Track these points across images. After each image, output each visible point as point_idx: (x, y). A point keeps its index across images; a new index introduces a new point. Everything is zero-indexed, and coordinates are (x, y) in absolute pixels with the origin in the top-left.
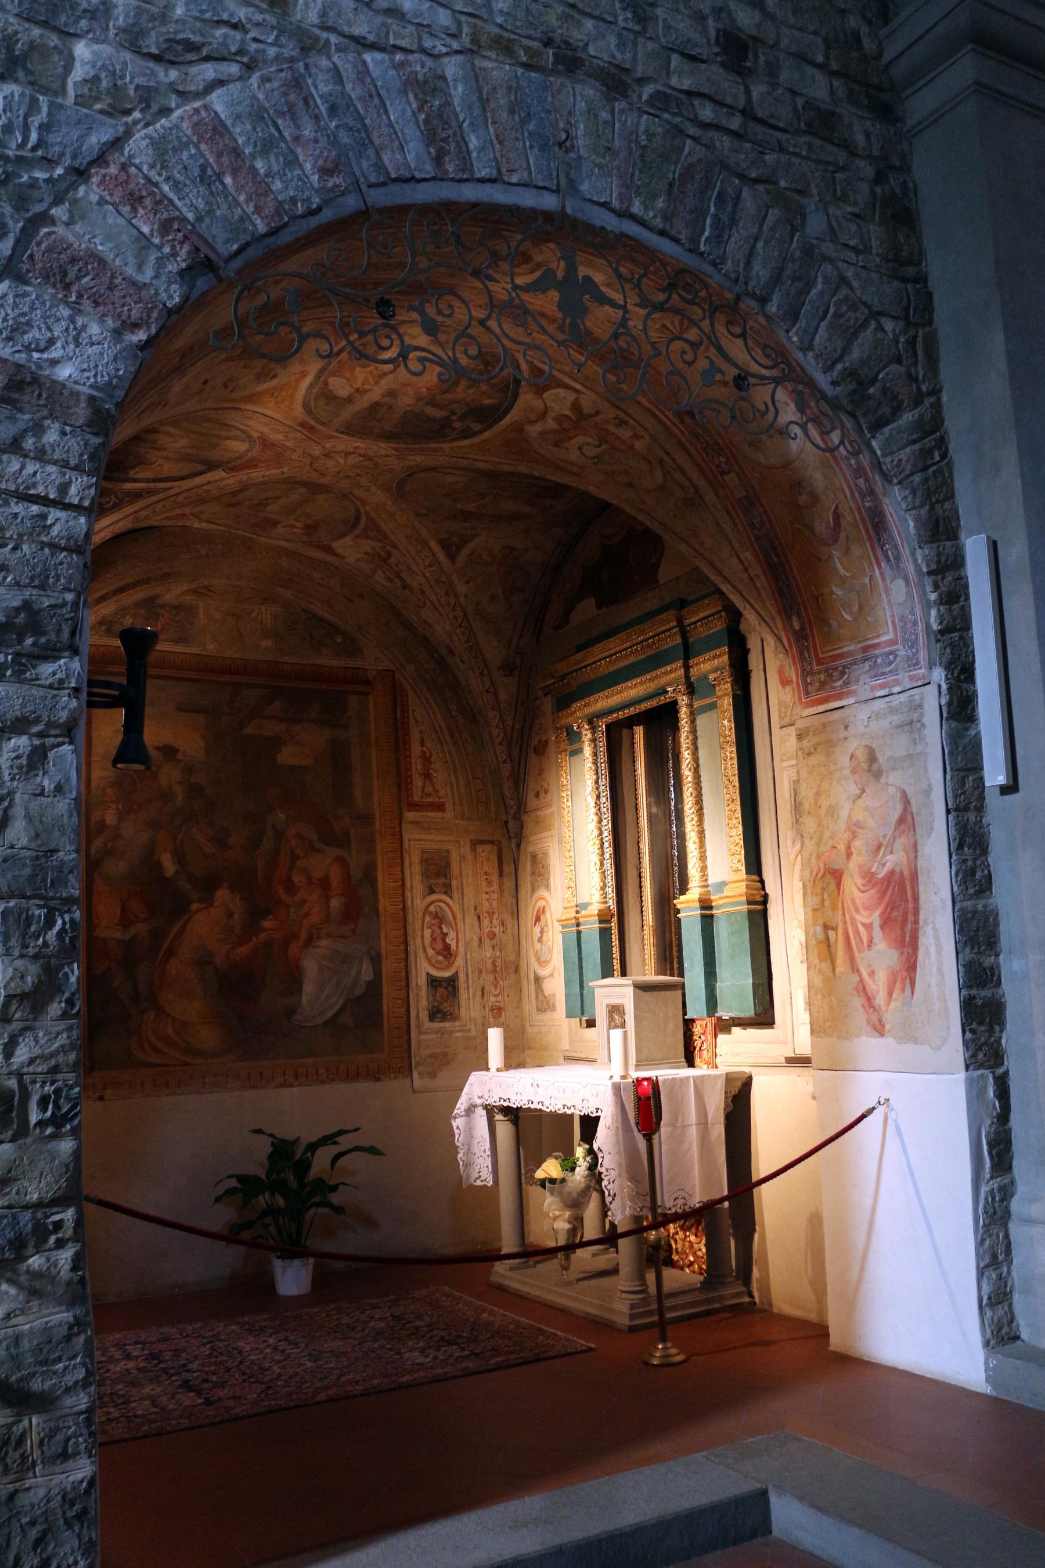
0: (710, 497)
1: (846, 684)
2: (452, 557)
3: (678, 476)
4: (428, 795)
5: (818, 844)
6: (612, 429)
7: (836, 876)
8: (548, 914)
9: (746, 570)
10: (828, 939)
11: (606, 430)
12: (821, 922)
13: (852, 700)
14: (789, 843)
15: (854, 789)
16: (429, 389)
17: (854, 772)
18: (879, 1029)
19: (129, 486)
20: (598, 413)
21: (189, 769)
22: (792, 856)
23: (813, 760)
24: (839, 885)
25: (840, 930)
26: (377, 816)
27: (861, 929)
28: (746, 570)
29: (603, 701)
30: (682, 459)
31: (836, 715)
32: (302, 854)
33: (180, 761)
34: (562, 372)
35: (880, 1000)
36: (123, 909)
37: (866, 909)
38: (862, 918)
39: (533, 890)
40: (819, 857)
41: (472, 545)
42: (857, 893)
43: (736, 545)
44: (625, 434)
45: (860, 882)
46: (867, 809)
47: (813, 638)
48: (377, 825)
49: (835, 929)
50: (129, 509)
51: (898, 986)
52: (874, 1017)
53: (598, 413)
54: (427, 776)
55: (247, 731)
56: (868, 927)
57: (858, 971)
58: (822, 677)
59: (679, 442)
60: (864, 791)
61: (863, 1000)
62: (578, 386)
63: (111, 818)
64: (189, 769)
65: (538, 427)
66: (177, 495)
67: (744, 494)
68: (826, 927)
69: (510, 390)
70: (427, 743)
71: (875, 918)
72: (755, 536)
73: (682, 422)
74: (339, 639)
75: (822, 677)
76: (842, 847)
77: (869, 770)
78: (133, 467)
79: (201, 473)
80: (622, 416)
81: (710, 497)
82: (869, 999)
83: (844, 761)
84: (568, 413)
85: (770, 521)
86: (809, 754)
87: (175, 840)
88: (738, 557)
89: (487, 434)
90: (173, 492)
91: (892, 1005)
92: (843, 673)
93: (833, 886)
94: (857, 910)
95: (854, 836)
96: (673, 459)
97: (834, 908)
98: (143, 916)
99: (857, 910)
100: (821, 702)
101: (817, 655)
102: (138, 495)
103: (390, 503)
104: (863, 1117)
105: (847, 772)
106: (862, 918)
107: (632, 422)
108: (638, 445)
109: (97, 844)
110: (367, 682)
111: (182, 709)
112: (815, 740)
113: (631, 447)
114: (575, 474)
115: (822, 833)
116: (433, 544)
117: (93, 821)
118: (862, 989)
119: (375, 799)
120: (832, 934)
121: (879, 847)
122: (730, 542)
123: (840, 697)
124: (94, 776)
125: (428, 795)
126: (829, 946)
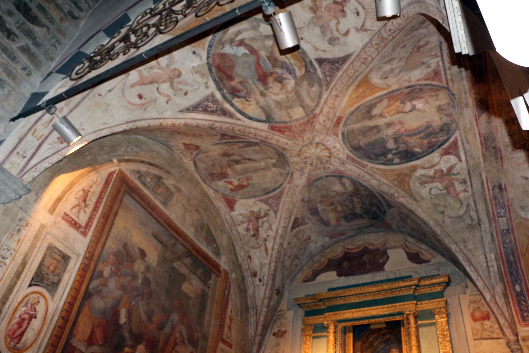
0: (485, 225)
2: (293, 228)
3: (473, 214)
4: (228, 338)
6: (456, 184)
9: (487, 262)
11: (453, 184)
16: (406, 131)
19: (227, 106)
20: (458, 174)
21: (148, 268)
26: (210, 338)
28: (487, 262)
29: (348, 314)
30: (481, 206)
32: (179, 344)
33: (146, 262)
34: (464, 148)
36: (92, 332)
41: (302, 227)
43: (487, 250)
44: (459, 187)
48: (209, 343)
50: (215, 118)
53: (458, 174)
54: (230, 328)
55: (175, 265)
59: (485, 200)
62: (463, 158)
63: (107, 271)
64: (148, 268)
65: (423, 172)
66: (239, 125)
67: (506, 227)
69: (431, 149)
70: (233, 312)
72: (504, 247)
73: (493, 190)
74: (215, 246)
78: (239, 97)
79: (260, 121)
80: (468, 179)
81: (485, 225)
84: (445, 170)
85: (515, 242)
87: (130, 303)
88: (485, 255)
89: (396, 167)
90: (239, 122)
96: (476, 205)
98: (100, 343)
102: (224, 113)
103: (301, 187)
107: (469, 183)
108: (462, 195)
109: (95, 283)
110: (219, 271)
111: (155, 236)
113: (458, 195)
114: (416, 201)
116: (293, 218)
117: (98, 269)
119: (211, 329)
122: (484, 248)
124: (108, 244)
125: (228, 338)
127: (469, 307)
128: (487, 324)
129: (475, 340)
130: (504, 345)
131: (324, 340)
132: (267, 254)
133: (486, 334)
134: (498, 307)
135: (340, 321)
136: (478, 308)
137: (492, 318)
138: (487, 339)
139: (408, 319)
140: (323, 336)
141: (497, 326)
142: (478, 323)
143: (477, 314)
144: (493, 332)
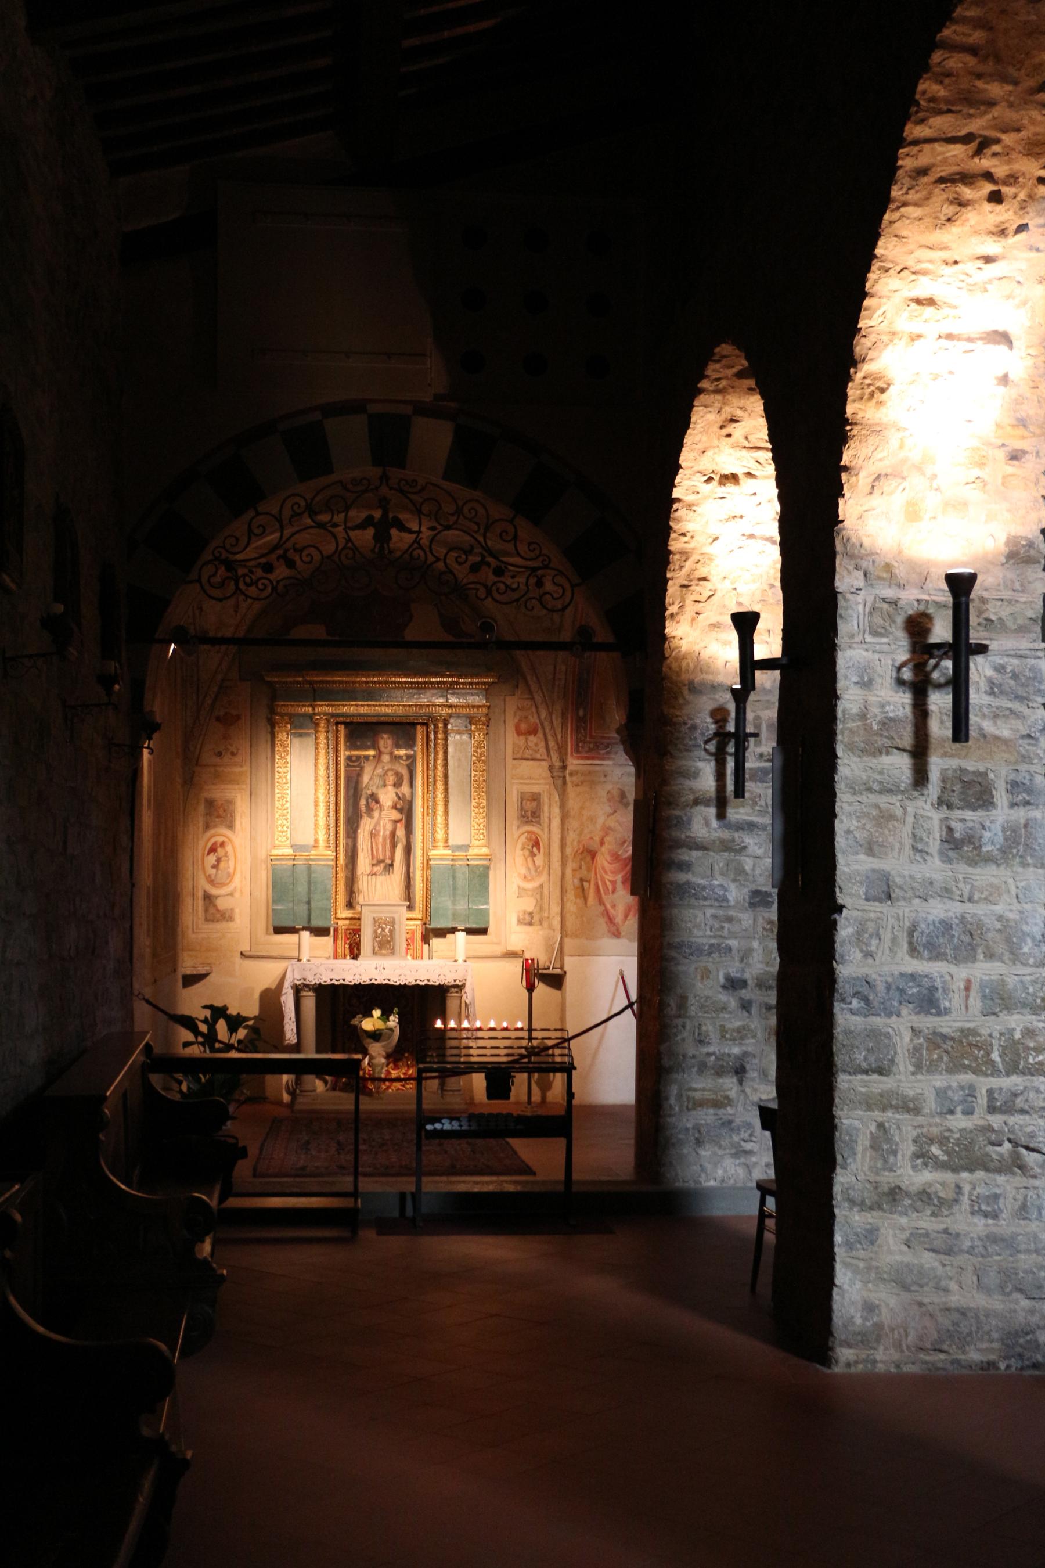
1: (608, 753)
5: (580, 834)
7: (593, 854)
8: (229, 848)
10: (582, 886)
12: (579, 876)
13: (610, 762)
14: (514, 828)
15: (609, 810)
17: (609, 800)
18: (617, 934)
22: (516, 836)
23: (579, 789)
24: (593, 858)
25: (592, 883)
27: (608, 883)
31: (598, 768)
35: (619, 919)
37: (612, 872)
38: (608, 877)
39: (207, 827)
40: (579, 842)
42: (606, 864)
45: (609, 858)
46: (617, 821)
47: (591, 723)
49: (589, 882)
51: (632, 913)
52: (614, 929)
56: (614, 883)
57: (604, 905)
58: (592, 746)
60: (615, 812)
61: (606, 919)
68: (582, 880)
71: (619, 878)
75: (592, 746)
76: (597, 839)
77: (621, 802)
82: (611, 920)
83: (604, 794)
86: (577, 785)
91: (627, 922)
92: (607, 747)
93: (589, 858)
94: (606, 872)
95: (607, 834)
97: (589, 870)
99: (606, 872)
100: (588, 758)
101: (590, 732)
104: (623, 978)
105: (605, 800)
106: (608, 877)
112: (582, 778)
115: (582, 830)
118: (607, 914)
120: (586, 884)
121: (624, 842)
123: (603, 759)
126: (583, 890)
127: (515, 716)
128: (532, 739)
129: (514, 759)
130: (546, 769)
131: (311, 740)
132: (236, 612)
133: (528, 754)
134: (552, 727)
135: (333, 715)
136: (526, 718)
137: (540, 734)
138: (528, 759)
139: (436, 727)
140: (308, 735)
141: (543, 744)
142: (521, 737)
143: (523, 726)
144: (537, 751)
